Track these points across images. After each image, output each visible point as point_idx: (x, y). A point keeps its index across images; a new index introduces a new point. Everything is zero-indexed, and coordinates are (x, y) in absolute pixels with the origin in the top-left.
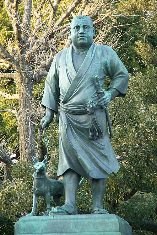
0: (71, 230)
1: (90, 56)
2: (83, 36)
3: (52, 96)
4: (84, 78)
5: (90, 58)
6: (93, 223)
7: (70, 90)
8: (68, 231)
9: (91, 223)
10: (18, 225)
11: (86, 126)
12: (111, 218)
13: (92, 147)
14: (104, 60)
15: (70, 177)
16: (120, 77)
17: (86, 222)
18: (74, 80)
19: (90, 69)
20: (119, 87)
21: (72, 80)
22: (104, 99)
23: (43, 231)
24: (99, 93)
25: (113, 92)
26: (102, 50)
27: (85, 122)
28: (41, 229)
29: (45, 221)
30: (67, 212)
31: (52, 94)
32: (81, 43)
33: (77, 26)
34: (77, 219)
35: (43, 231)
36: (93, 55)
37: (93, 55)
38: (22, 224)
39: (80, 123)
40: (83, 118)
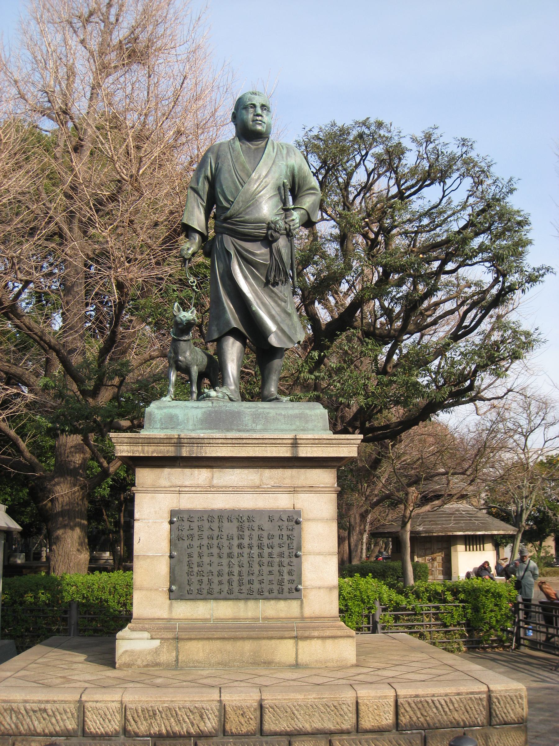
0: (246, 425)
5: (272, 153)
6: (284, 415)
8: (240, 427)
9: (280, 414)
10: (150, 414)
12: (314, 409)
13: (271, 297)
15: (233, 343)
17: (273, 413)
20: (309, 208)
25: (302, 214)
28: (191, 422)
29: (198, 410)
34: (254, 408)
35: (195, 425)
36: (275, 150)
37: (275, 150)
38: (156, 411)
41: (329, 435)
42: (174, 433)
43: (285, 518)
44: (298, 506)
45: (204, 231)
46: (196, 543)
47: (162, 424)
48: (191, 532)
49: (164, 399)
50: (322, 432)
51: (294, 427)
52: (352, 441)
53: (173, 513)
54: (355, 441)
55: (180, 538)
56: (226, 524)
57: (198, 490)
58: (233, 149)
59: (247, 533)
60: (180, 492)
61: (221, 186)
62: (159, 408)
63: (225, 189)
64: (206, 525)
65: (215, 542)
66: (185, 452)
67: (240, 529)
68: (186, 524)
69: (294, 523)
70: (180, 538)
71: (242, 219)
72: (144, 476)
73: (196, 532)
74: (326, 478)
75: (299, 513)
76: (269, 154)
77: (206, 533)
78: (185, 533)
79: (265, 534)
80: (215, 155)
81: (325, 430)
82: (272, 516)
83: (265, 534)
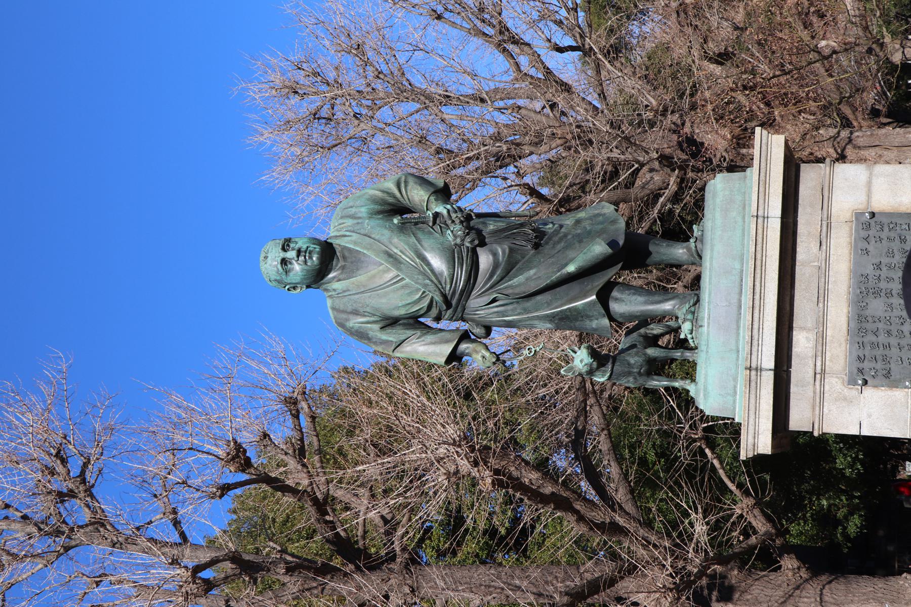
1: (349, 238)
2: (305, 252)
3: (430, 338)
4: (395, 251)
7: (419, 281)
11: (504, 252)
14: (363, 211)
15: (616, 299)
16: (406, 186)
18: (398, 269)
19: (377, 238)
21: (398, 276)
22: (448, 211)
23: (731, 350)
24: (434, 223)
26: (342, 218)
27: (495, 255)
30: (695, 304)
31: (423, 338)
32: (318, 258)
33: (281, 263)
36: (348, 233)
37: (348, 233)
39: (496, 265)
40: (485, 260)
41: (753, 173)
42: (743, 374)
43: (864, 234)
44: (848, 215)
45: (456, 337)
46: (895, 351)
47: (728, 394)
48: (879, 358)
49: (692, 394)
50: (747, 181)
51: (740, 219)
52: (764, 142)
53: (852, 382)
54: (764, 138)
55: (888, 375)
56: (868, 312)
57: (820, 348)
58: (344, 291)
59: (883, 285)
60: (823, 372)
61: (398, 308)
62: (706, 397)
63: (404, 303)
64: (871, 338)
65: (894, 329)
66: (769, 361)
67: (877, 293)
68: (867, 365)
69: (872, 222)
70: (888, 375)
71: (448, 281)
72: (798, 420)
73: (879, 352)
74: (809, 176)
75: (858, 215)
76: (355, 243)
77: (882, 339)
78: (879, 365)
79: (885, 260)
80: (351, 316)
81: (745, 177)
82: (861, 248)
83: (885, 260)
